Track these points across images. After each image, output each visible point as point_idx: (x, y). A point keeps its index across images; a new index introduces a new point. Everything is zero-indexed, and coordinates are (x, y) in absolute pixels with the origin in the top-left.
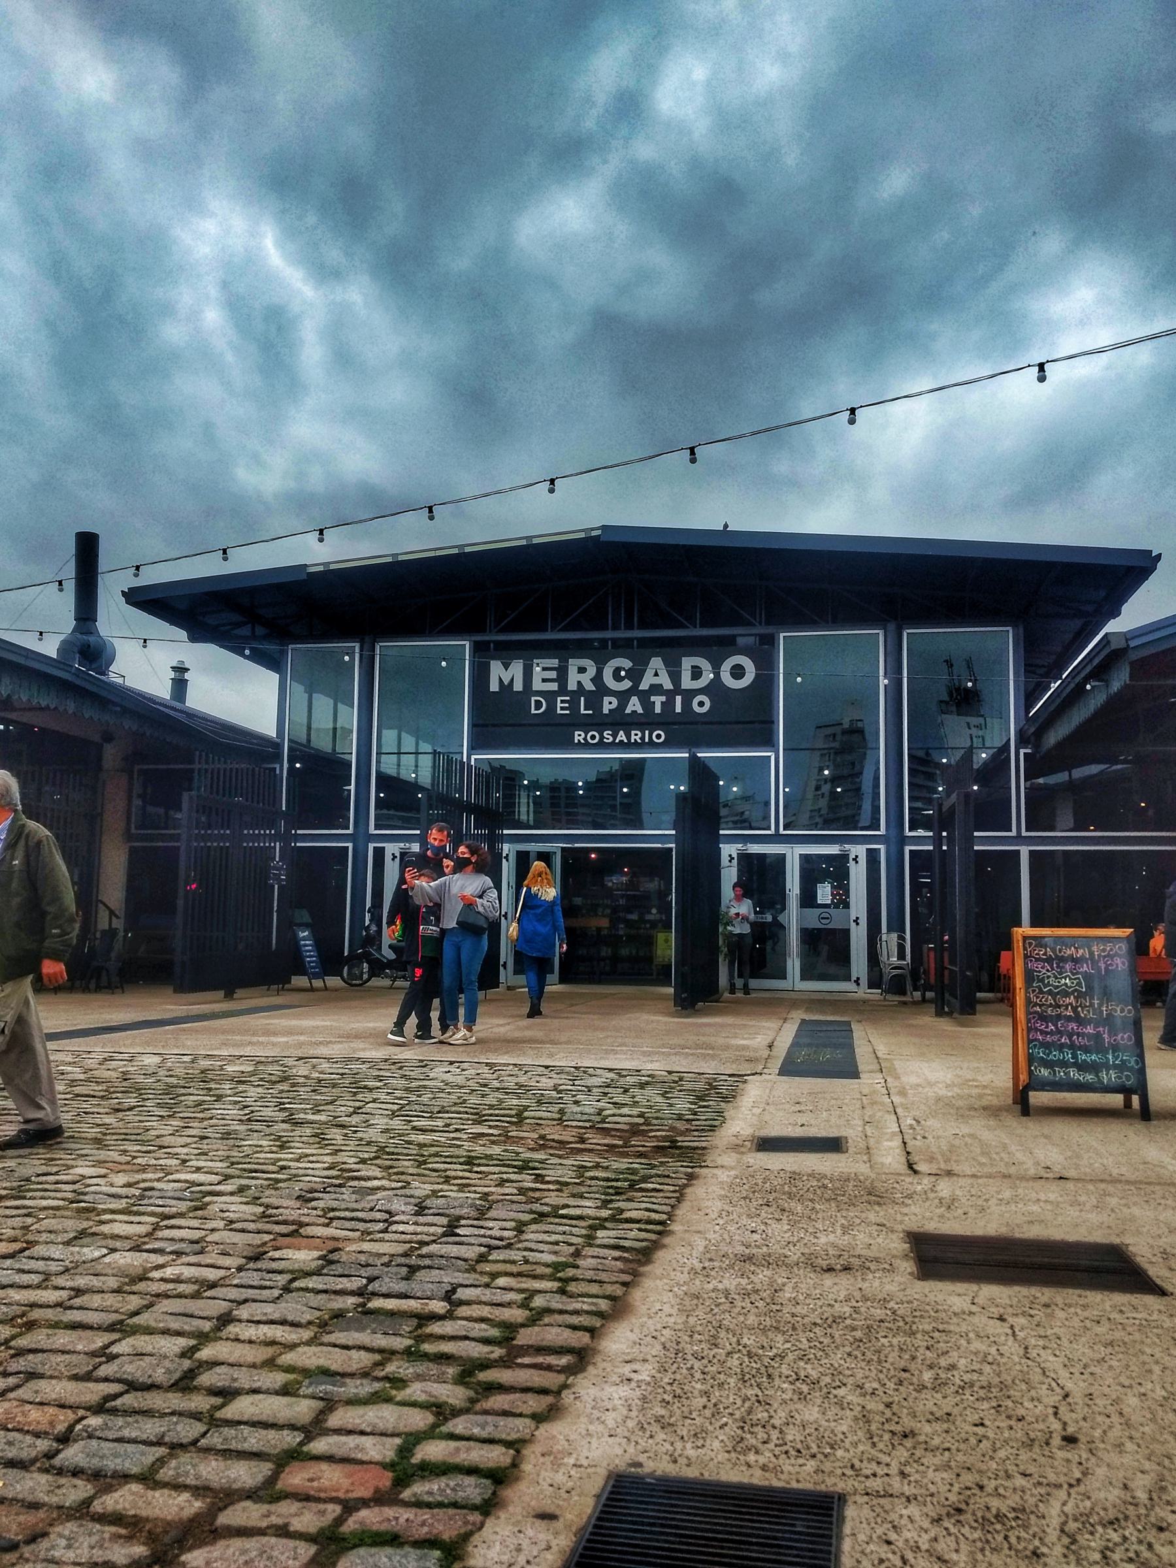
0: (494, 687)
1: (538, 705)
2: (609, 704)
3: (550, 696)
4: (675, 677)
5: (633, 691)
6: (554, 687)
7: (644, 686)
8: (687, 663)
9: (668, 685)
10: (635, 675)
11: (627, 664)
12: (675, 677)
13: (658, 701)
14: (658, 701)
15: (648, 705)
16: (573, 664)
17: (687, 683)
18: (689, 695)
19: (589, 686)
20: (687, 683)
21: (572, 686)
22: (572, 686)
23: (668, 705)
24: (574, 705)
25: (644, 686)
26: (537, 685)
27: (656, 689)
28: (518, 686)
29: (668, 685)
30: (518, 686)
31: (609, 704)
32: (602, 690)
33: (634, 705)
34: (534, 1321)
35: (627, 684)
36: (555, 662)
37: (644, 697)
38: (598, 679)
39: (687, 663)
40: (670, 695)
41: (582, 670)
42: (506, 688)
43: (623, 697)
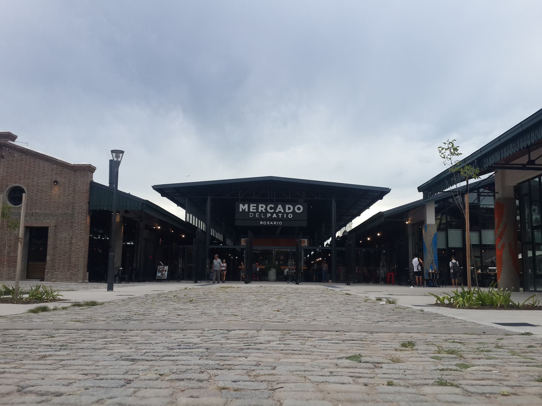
0: (241, 210)
1: (251, 215)
2: (269, 215)
3: (254, 213)
4: (284, 209)
5: (274, 212)
6: (255, 211)
7: (277, 211)
8: (287, 206)
9: (283, 211)
10: (275, 208)
11: (273, 206)
12: (284, 209)
13: (280, 215)
14: (280, 215)
15: (278, 216)
16: (260, 206)
17: (287, 211)
18: (288, 213)
19: (264, 211)
20: (287, 211)
21: (260, 211)
22: (260, 211)
23: (283, 216)
24: (260, 215)
25: (277, 211)
26: (251, 210)
27: (280, 212)
28: (247, 210)
29: (283, 211)
30: (247, 210)
31: (269, 215)
32: (267, 212)
33: (275, 216)
34: (398, 393)
35: (273, 211)
36: (255, 205)
37: (277, 214)
38: (266, 209)
39: (287, 206)
40: (283, 214)
41: (262, 207)
42: (244, 211)
43: (272, 214)
